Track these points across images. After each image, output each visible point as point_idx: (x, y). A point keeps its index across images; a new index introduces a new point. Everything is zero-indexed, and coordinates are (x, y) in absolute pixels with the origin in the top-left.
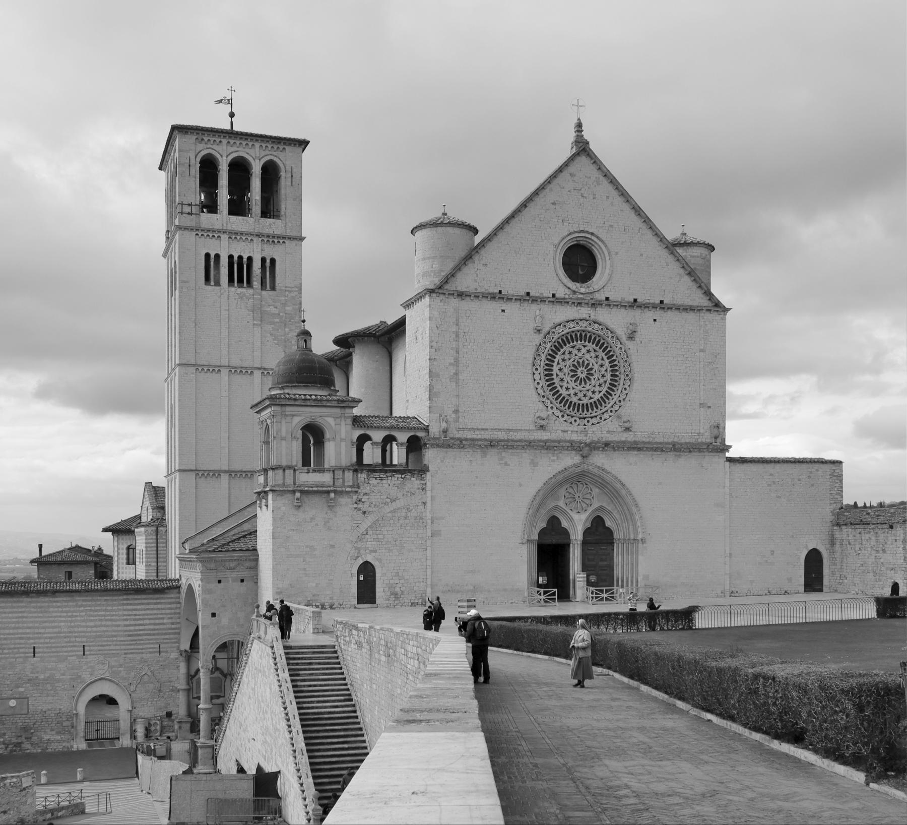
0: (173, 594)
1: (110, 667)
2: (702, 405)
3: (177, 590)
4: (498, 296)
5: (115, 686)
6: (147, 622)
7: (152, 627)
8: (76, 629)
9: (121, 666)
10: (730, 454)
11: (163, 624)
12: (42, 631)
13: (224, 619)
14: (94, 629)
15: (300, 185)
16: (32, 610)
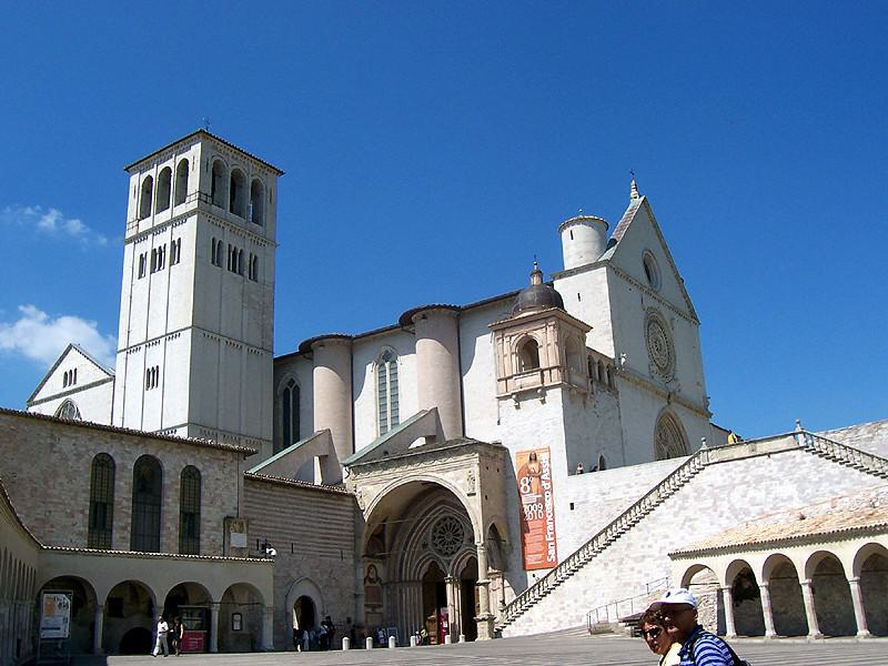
0: (349, 502)
1: (311, 568)
2: (698, 383)
3: (351, 499)
4: (628, 278)
5: (311, 585)
6: (334, 526)
7: (337, 532)
8: (286, 526)
9: (317, 567)
10: (711, 421)
11: (343, 530)
12: (263, 523)
13: (492, 502)
14: (300, 528)
15: (276, 204)
16: (256, 501)
